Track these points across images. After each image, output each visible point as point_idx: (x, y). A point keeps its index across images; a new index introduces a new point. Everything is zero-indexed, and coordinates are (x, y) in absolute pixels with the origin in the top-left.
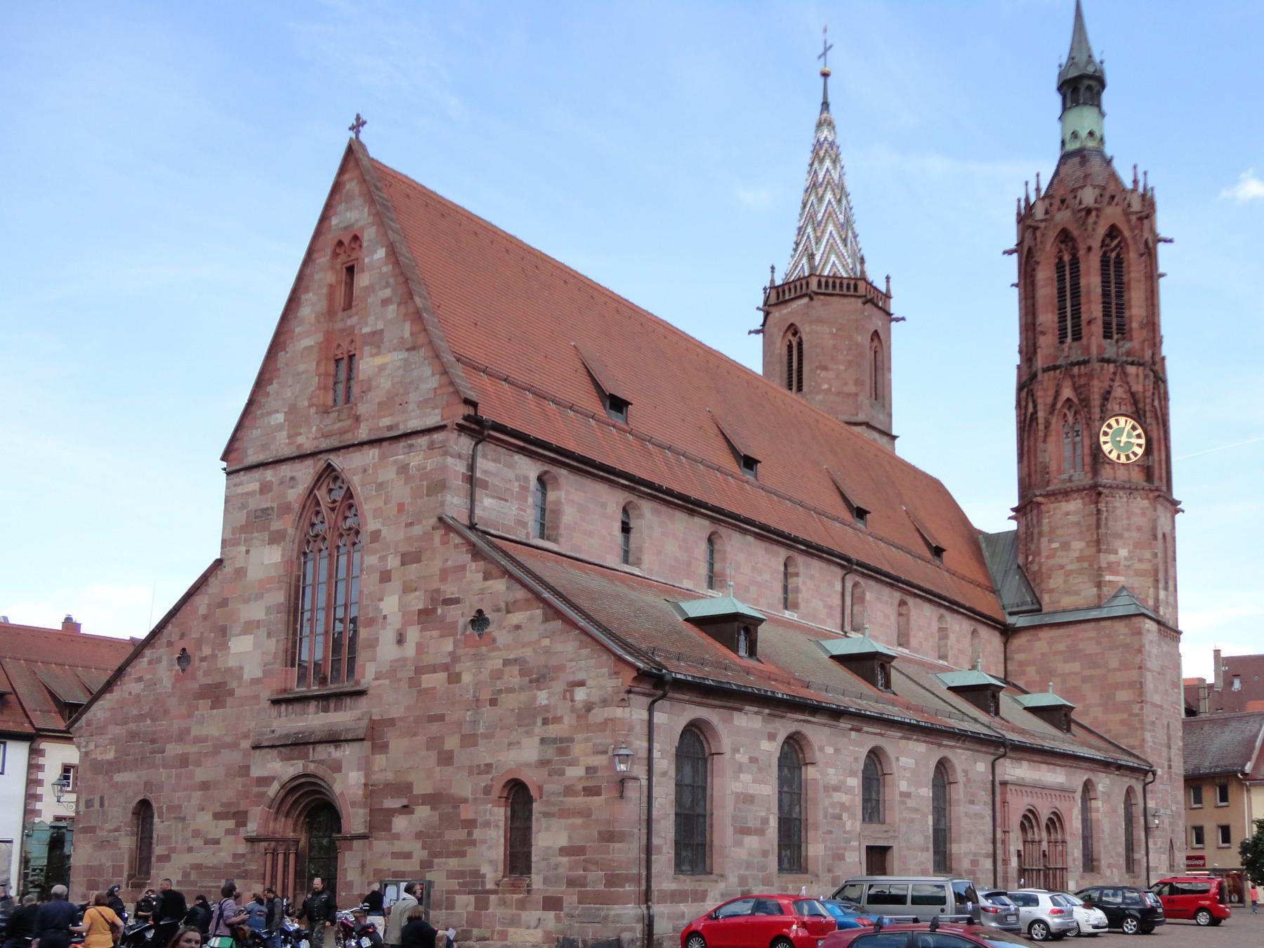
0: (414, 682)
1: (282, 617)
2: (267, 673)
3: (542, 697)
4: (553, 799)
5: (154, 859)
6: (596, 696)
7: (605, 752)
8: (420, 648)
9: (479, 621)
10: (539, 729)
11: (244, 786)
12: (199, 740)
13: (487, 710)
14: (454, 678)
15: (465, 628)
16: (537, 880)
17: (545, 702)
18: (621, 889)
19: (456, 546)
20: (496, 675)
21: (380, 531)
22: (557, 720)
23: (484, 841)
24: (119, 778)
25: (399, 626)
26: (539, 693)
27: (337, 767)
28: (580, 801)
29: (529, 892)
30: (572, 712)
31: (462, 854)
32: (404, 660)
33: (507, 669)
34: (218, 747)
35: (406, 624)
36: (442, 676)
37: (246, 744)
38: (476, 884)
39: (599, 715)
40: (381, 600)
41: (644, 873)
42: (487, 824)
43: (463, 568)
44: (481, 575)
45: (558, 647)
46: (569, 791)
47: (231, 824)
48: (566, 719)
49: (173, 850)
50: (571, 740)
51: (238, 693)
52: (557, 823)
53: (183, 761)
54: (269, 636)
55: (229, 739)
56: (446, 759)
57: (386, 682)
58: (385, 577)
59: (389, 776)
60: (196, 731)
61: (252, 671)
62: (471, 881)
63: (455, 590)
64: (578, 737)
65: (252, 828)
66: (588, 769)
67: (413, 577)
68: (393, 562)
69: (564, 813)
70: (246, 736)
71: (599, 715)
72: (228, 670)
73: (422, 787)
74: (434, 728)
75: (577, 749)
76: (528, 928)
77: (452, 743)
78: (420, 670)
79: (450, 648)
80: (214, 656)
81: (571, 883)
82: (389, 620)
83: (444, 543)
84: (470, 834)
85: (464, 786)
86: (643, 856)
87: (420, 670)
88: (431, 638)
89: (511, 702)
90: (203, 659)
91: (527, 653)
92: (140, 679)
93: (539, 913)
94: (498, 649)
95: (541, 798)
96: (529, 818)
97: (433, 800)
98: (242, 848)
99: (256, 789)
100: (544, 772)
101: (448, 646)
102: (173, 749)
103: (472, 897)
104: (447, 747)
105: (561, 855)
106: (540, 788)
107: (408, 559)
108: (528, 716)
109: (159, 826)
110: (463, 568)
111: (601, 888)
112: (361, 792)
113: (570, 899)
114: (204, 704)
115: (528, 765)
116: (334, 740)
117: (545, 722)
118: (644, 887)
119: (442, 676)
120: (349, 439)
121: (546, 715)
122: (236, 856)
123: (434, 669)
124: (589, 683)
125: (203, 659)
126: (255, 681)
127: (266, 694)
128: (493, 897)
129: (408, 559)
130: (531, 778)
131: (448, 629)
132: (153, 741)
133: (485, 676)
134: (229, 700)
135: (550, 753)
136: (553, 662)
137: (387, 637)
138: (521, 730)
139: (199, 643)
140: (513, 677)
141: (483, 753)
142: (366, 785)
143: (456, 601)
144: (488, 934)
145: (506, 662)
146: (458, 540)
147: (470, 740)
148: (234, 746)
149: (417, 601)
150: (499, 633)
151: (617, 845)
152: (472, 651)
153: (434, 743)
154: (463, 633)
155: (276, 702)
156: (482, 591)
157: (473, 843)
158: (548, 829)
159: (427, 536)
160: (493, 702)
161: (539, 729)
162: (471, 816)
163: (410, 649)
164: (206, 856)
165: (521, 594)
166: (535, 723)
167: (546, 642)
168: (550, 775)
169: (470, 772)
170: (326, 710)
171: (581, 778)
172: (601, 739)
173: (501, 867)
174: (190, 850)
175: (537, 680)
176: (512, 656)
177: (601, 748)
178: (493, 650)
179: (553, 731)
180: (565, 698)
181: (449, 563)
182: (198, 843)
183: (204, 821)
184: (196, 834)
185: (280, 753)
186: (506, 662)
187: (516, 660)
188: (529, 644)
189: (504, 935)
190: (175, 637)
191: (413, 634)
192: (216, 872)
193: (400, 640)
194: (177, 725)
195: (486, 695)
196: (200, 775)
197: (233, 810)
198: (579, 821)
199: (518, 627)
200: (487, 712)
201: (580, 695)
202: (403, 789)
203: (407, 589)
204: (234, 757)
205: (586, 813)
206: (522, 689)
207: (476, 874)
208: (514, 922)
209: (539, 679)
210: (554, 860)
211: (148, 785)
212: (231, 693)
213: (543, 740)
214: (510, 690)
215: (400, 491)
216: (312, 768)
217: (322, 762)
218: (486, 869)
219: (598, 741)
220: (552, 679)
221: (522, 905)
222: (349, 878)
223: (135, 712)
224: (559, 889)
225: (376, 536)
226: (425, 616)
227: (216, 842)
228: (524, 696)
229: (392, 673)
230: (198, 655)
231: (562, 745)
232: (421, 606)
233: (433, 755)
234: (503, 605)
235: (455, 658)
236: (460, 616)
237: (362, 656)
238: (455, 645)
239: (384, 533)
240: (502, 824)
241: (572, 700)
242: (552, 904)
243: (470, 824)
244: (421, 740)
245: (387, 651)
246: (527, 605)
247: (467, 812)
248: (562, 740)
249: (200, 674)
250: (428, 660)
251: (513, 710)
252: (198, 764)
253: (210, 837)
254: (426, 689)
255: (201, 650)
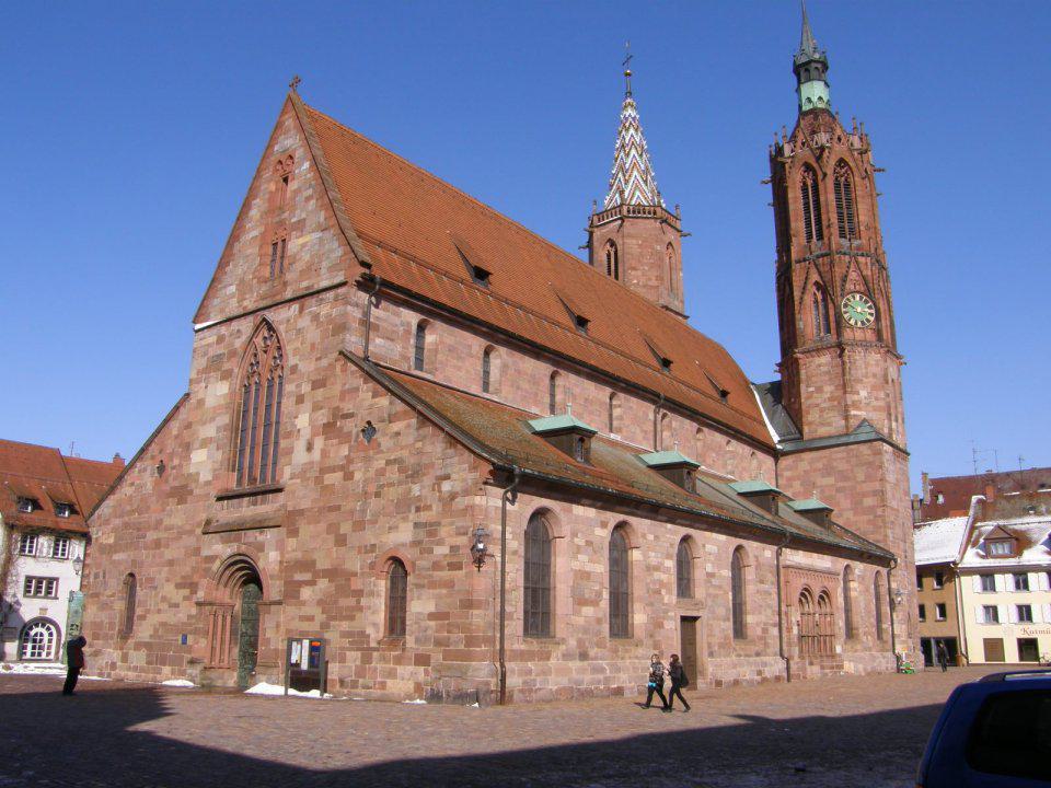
0: (319, 480)
1: (227, 433)
2: (216, 477)
3: (416, 490)
4: (424, 573)
5: (135, 618)
6: (458, 487)
7: (465, 534)
8: (324, 453)
9: (369, 430)
10: (412, 516)
11: (197, 563)
12: (168, 529)
13: (373, 501)
14: (349, 476)
15: (358, 436)
16: (410, 640)
17: (418, 494)
18: (478, 649)
19: (352, 373)
20: (381, 472)
21: (296, 365)
22: (428, 508)
23: (369, 608)
24: (116, 557)
25: (308, 437)
26: (413, 486)
27: (261, 548)
28: (445, 574)
29: (404, 650)
30: (440, 501)
31: (352, 618)
32: (311, 463)
33: (389, 468)
34: (181, 533)
35: (314, 434)
36: (339, 475)
37: (199, 531)
38: (363, 642)
39: (461, 502)
40: (296, 417)
41: (498, 635)
42: (372, 594)
43: (357, 389)
44: (370, 394)
45: (429, 448)
46: (436, 566)
47: (186, 592)
48: (434, 508)
49: (148, 611)
50: (439, 524)
51: (197, 491)
52: (427, 593)
53: (157, 544)
54: (218, 449)
55: (188, 527)
56: (341, 541)
57: (299, 481)
58: (300, 399)
59: (299, 555)
60: (167, 522)
61: (205, 476)
62: (359, 640)
63: (351, 406)
64: (444, 521)
65: (201, 595)
66: (451, 547)
67: (320, 399)
68: (306, 388)
69: (433, 585)
70: (199, 525)
71: (461, 502)
72: (190, 475)
73: (323, 563)
74: (332, 517)
75: (443, 532)
76: (403, 679)
77: (345, 528)
78: (324, 471)
79: (347, 453)
80: (180, 466)
81: (438, 643)
82: (302, 432)
83: (344, 370)
84: (358, 602)
85: (355, 563)
86: (498, 621)
87: (324, 471)
88: (332, 445)
89: (393, 493)
90: (174, 468)
91: (405, 454)
92: (132, 484)
93: (411, 668)
94: (382, 452)
95: (414, 572)
96: (404, 590)
97: (331, 574)
98: (194, 611)
99: (204, 566)
100: (417, 550)
101: (345, 451)
102: (151, 536)
103: (359, 653)
104: (342, 532)
105: (429, 620)
106: (414, 564)
107: (316, 385)
108: (405, 505)
109: (140, 593)
110: (357, 389)
111: (462, 647)
112: (277, 568)
113: (437, 657)
114: (172, 504)
115: (403, 545)
116: (260, 526)
117: (418, 509)
118: (498, 647)
119: (339, 475)
120: (278, 298)
121: (418, 504)
122: (190, 617)
123: (333, 470)
124: (454, 476)
125: (174, 468)
126: (208, 483)
127: (214, 493)
128: (375, 654)
129: (316, 385)
130: (406, 555)
131: (344, 437)
132: (139, 530)
133: (371, 473)
134: (189, 498)
135: (422, 534)
136: (425, 460)
137: (300, 445)
138: (399, 516)
139: (172, 455)
140: (393, 474)
141: (369, 537)
142: (281, 562)
143: (351, 415)
144: (371, 684)
145: (388, 462)
146: (354, 368)
147: (359, 526)
148: (191, 532)
149: (323, 417)
150: (384, 441)
151: (475, 612)
152: (362, 454)
153: (333, 528)
154: (356, 441)
155: (220, 499)
156: (371, 407)
157: (361, 609)
158: (419, 599)
159: (331, 366)
160: (378, 495)
161: (412, 516)
162: (360, 587)
163: (316, 455)
164: (171, 617)
165: (400, 406)
166: (410, 511)
167: (419, 444)
168: (421, 553)
169: (359, 552)
170: (255, 504)
171: (446, 556)
172: (460, 523)
173: (382, 629)
174: (159, 611)
175: (412, 476)
176: (392, 457)
177: (462, 531)
178: (378, 453)
179: (424, 516)
180: (434, 490)
181: (347, 386)
182: (164, 606)
183: (169, 590)
184: (164, 599)
185: (222, 537)
186: (388, 462)
187: (395, 460)
188: (407, 446)
189: (383, 685)
190: (156, 452)
191: (319, 443)
192: (174, 628)
193: (310, 448)
194: (154, 517)
195: (372, 488)
196: (168, 554)
197: (189, 581)
198: (444, 591)
199: (398, 434)
200: (373, 503)
201: (446, 486)
202: (306, 565)
203: (316, 407)
204: (190, 541)
205: (450, 584)
206: (400, 483)
207: (363, 635)
208: (392, 674)
209: (415, 475)
210: (423, 624)
211: (134, 562)
212: (191, 492)
213: (416, 525)
214: (392, 485)
215: (313, 334)
216: (243, 548)
217: (248, 544)
218: (370, 630)
219: (460, 524)
220: (424, 475)
221: (399, 661)
222: (268, 635)
223: (128, 508)
224: (429, 648)
225: (294, 369)
226: (329, 429)
227: (177, 606)
228: (400, 490)
229: (302, 474)
230: (170, 465)
231: (431, 529)
232: (325, 421)
233: (331, 538)
234: (386, 416)
235: (349, 460)
236: (353, 427)
237: (282, 461)
238: (350, 451)
239: (299, 367)
240: (383, 594)
241: (440, 491)
242: (422, 660)
243: (359, 593)
244: (322, 526)
245: (300, 456)
246: (404, 415)
247: (356, 584)
248: (431, 525)
249: (171, 479)
250: (330, 462)
251: (393, 501)
252: (167, 546)
253: (173, 601)
254: (327, 486)
255: (172, 460)
